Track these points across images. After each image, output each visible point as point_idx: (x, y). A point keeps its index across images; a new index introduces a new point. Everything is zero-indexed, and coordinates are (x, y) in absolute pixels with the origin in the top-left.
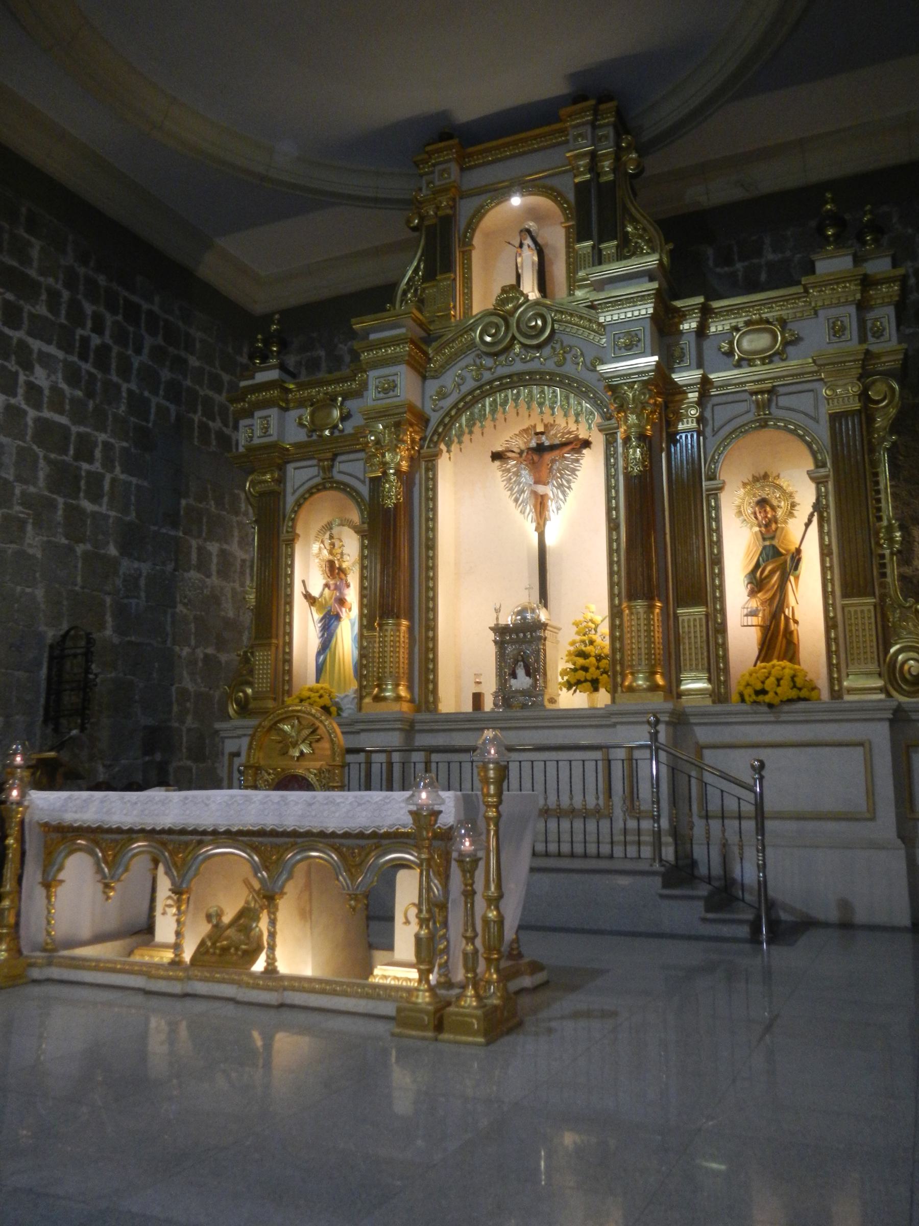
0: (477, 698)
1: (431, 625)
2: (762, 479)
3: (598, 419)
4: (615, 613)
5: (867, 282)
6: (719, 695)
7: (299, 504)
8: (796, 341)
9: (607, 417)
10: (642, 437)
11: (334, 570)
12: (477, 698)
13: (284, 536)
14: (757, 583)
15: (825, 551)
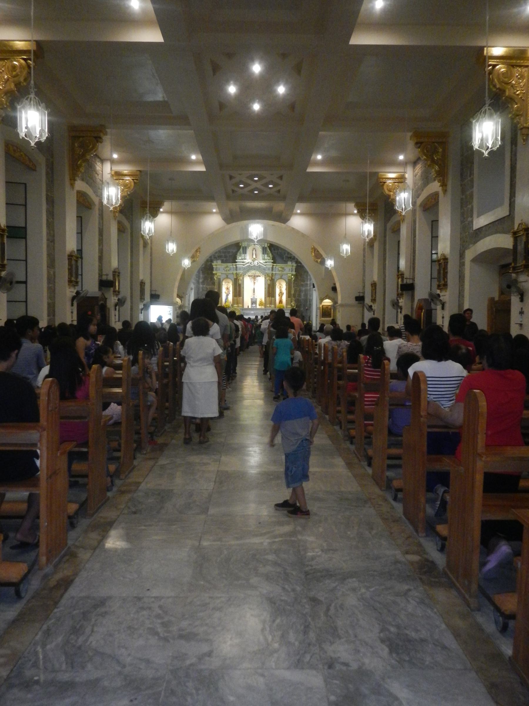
0: (248, 306)
1: (243, 298)
2: (280, 284)
3: (264, 276)
4: (265, 298)
5: (292, 266)
6: (275, 307)
7: (223, 280)
8: (285, 270)
9: (265, 276)
10: (270, 280)
11: (228, 289)
12: (248, 306)
13: (221, 284)
14: (279, 295)
15: (286, 293)
